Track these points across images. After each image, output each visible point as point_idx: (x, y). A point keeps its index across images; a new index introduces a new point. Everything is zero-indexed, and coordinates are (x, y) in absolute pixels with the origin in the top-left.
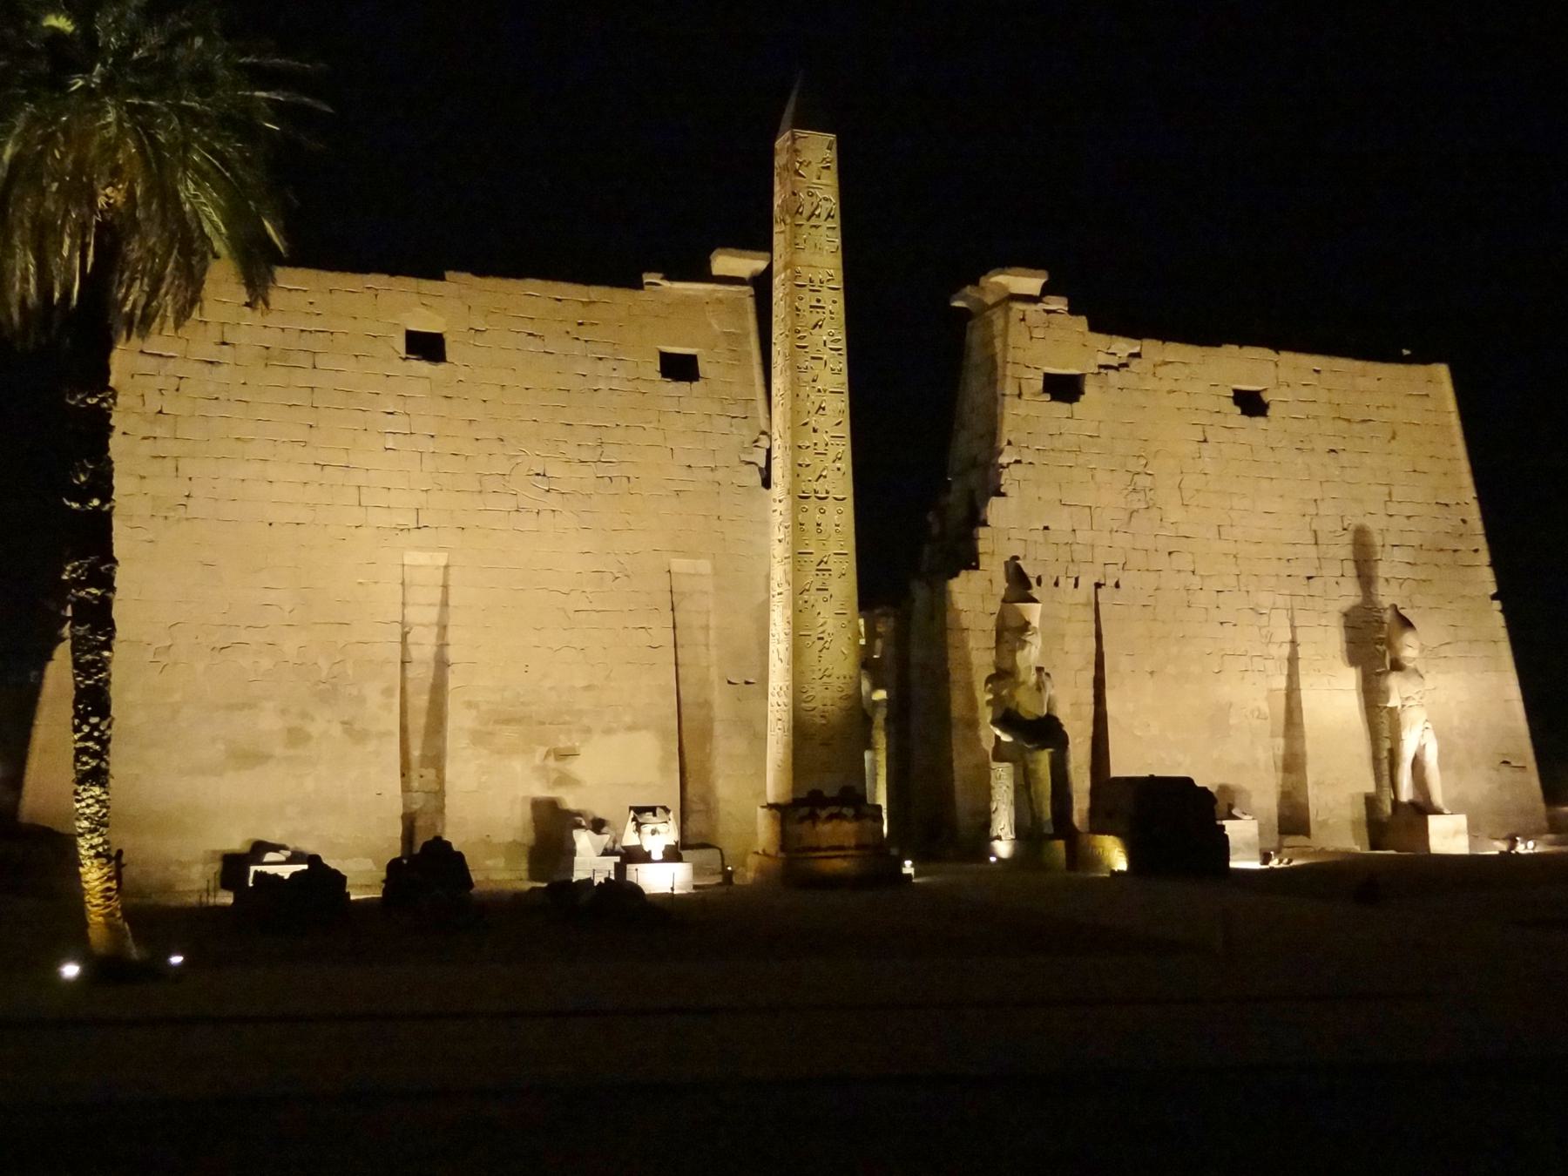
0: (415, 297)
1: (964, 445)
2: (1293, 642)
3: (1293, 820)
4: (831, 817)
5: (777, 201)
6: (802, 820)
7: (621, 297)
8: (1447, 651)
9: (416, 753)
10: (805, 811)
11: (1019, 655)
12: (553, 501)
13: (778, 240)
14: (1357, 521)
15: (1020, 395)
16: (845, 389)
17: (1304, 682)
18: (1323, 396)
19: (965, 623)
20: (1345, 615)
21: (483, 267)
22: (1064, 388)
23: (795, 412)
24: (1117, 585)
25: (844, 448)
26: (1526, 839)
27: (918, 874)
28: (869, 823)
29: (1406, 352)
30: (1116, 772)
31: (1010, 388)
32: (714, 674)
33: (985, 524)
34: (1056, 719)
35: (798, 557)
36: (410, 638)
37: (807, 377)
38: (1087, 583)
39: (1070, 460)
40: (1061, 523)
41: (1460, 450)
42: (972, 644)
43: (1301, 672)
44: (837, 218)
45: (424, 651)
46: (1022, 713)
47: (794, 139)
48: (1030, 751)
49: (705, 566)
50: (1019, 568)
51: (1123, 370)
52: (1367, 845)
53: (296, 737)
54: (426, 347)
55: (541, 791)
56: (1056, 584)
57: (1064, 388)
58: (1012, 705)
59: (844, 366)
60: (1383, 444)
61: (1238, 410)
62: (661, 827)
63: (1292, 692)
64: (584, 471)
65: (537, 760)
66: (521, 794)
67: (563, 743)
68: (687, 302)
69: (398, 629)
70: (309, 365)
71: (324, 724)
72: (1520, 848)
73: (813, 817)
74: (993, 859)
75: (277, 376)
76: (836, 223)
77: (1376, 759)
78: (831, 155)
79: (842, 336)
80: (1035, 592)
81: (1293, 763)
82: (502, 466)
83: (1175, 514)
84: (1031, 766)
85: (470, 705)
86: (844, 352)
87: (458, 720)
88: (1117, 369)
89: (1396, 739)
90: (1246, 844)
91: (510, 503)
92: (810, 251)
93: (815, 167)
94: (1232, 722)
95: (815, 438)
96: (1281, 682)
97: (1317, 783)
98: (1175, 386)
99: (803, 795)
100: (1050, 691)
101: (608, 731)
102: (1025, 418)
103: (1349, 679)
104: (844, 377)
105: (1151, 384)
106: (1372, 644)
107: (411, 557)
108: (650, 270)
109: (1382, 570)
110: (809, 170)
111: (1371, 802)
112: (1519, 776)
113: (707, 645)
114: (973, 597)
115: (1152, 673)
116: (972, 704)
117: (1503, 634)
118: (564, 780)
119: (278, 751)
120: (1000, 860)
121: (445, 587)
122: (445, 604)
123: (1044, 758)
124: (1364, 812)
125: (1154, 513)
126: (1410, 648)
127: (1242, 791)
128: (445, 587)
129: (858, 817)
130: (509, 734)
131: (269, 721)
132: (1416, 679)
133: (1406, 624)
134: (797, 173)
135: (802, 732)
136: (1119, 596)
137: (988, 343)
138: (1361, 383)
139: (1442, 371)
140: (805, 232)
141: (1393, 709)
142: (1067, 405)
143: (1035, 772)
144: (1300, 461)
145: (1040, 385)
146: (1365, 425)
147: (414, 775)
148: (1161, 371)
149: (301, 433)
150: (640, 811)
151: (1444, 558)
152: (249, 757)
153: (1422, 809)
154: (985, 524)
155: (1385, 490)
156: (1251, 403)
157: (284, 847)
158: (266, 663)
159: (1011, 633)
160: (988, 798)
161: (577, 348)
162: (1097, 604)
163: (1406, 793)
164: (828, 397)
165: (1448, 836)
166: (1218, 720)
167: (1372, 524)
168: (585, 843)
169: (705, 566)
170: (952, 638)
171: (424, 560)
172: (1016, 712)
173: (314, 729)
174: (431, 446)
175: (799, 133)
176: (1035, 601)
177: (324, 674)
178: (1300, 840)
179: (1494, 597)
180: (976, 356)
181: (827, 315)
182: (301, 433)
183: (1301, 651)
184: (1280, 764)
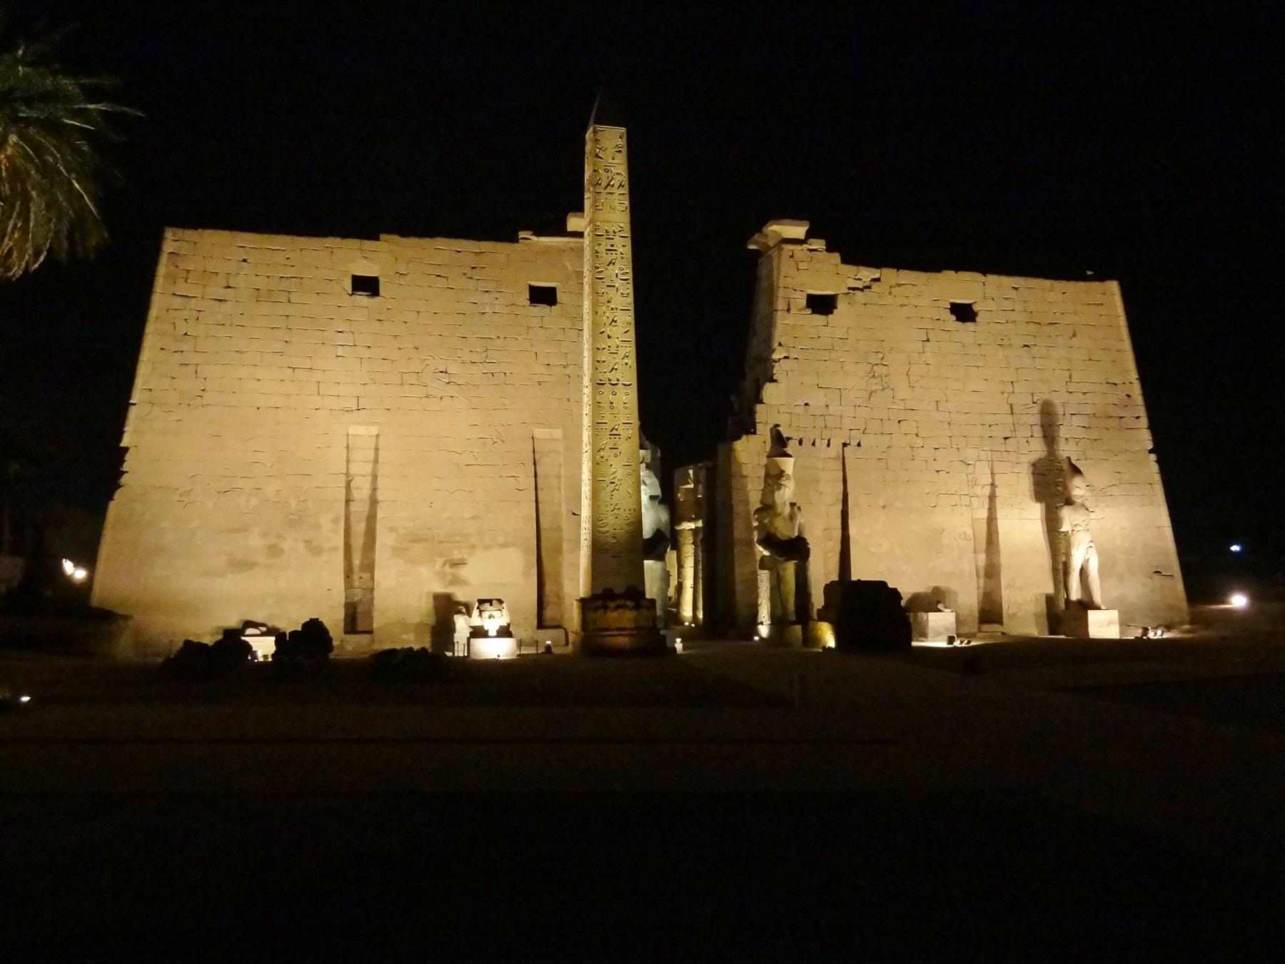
0: (359, 253)
1: (755, 346)
2: (993, 485)
3: (990, 613)
4: (618, 607)
5: (586, 177)
6: (597, 609)
7: (502, 248)
8: (1114, 491)
9: (356, 562)
10: (599, 603)
11: (776, 494)
12: (452, 390)
13: (587, 204)
14: (1046, 397)
15: (788, 310)
16: (631, 307)
17: (1000, 514)
18: (1019, 307)
19: (745, 472)
20: (1034, 465)
21: (405, 233)
22: (822, 305)
23: (595, 325)
24: (859, 445)
25: (631, 349)
26: (1155, 628)
27: (684, 648)
28: (644, 612)
29: (1089, 273)
31: (780, 305)
32: (564, 509)
33: (761, 402)
35: (597, 425)
36: (353, 485)
37: (602, 299)
39: (826, 355)
40: (817, 400)
41: (1127, 345)
42: (750, 487)
43: (998, 506)
44: (627, 186)
45: (361, 491)
46: (779, 536)
47: (595, 132)
48: (781, 563)
49: (558, 433)
50: (779, 434)
51: (866, 291)
52: (1046, 629)
53: (274, 551)
54: (367, 285)
55: (440, 589)
56: (813, 444)
57: (822, 305)
59: (631, 291)
60: (1066, 343)
61: (954, 318)
62: (496, 614)
63: (991, 520)
64: (474, 368)
65: (438, 567)
66: (426, 590)
67: (456, 555)
68: (547, 250)
69: (344, 478)
70: (285, 300)
71: (292, 543)
72: (1151, 635)
73: (605, 608)
74: (756, 638)
75: (264, 308)
76: (625, 191)
77: (1055, 570)
78: (622, 142)
79: (629, 270)
80: (789, 450)
81: (991, 572)
82: (416, 366)
83: (903, 392)
85: (391, 529)
86: (631, 281)
87: (384, 540)
88: (862, 290)
89: (1068, 555)
90: (938, 630)
91: (423, 391)
92: (607, 213)
93: (611, 151)
94: (945, 541)
95: (609, 342)
96: (984, 514)
97: (1010, 586)
98: (905, 301)
99: (599, 591)
100: (800, 519)
101: (487, 548)
102: (791, 327)
103: (1036, 511)
104: (631, 299)
105: (889, 300)
106: (1052, 485)
107: (354, 430)
108: (524, 229)
109: (1063, 432)
110: (608, 154)
111: (1050, 600)
112: (1167, 582)
113: (560, 489)
114: (749, 452)
116: (750, 529)
117: (1157, 478)
118: (456, 581)
119: (262, 560)
120: (762, 639)
121: (377, 449)
122: (376, 461)
123: (790, 568)
124: (1045, 610)
126: (1078, 489)
127: (949, 591)
128: (377, 449)
129: (637, 607)
130: (419, 549)
131: (255, 541)
132: (1083, 511)
133: (1077, 471)
134: (597, 156)
135: (598, 548)
136: (860, 451)
137: (770, 275)
138: (1051, 296)
139: (1114, 286)
140: (604, 195)
141: (1066, 534)
142: (823, 317)
144: (1001, 353)
145: (804, 302)
146: (1052, 327)
147: (356, 577)
148: (895, 291)
149: (279, 347)
150: (481, 602)
151: (1113, 423)
152: (241, 564)
153: (1087, 604)
154: (761, 402)
155: (1067, 373)
156: (964, 313)
157: (263, 625)
158: (254, 501)
159: (774, 478)
160: (757, 597)
161: (471, 285)
163: (1075, 594)
164: (619, 313)
165: (1103, 626)
166: (934, 540)
167: (1057, 400)
168: (462, 625)
169: (558, 433)
170: (734, 482)
171: (362, 431)
172: (775, 535)
173: (286, 545)
174: (367, 353)
175: (599, 127)
176: (790, 456)
177: (293, 507)
178: (996, 627)
179: (1151, 451)
180: (764, 284)
181: (619, 256)
182: (279, 347)
183: (998, 491)
184: (982, 572)
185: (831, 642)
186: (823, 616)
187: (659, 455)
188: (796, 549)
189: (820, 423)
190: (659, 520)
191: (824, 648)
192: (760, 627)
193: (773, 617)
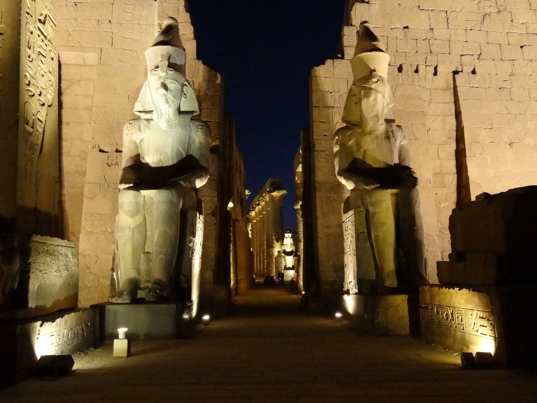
19: (330, 103)
24: (474, 72)
30: (474, 194)
34: (408, 169)
38: (445, 70)
46: (369, 161)
48: (369, 192)
49: (92, 57)
56: (417, 71)
58: (360, 156)
80: (380, 44)
84: (371, 209)
100: (400, 141)
115: (511, 144)
123: (385, 200)
125: (506, 16)
136: (474, 80)
143: (374, 214)
162: (455, 88)
170: (316, 113)
185: (483, 341)
186: (454, 275)
187: (219, 81)
188: (400, 178)
189: (423, 47)
190: (189, 144)
191: (467, 357)
192: (346, 297)
193: (360, 282)
